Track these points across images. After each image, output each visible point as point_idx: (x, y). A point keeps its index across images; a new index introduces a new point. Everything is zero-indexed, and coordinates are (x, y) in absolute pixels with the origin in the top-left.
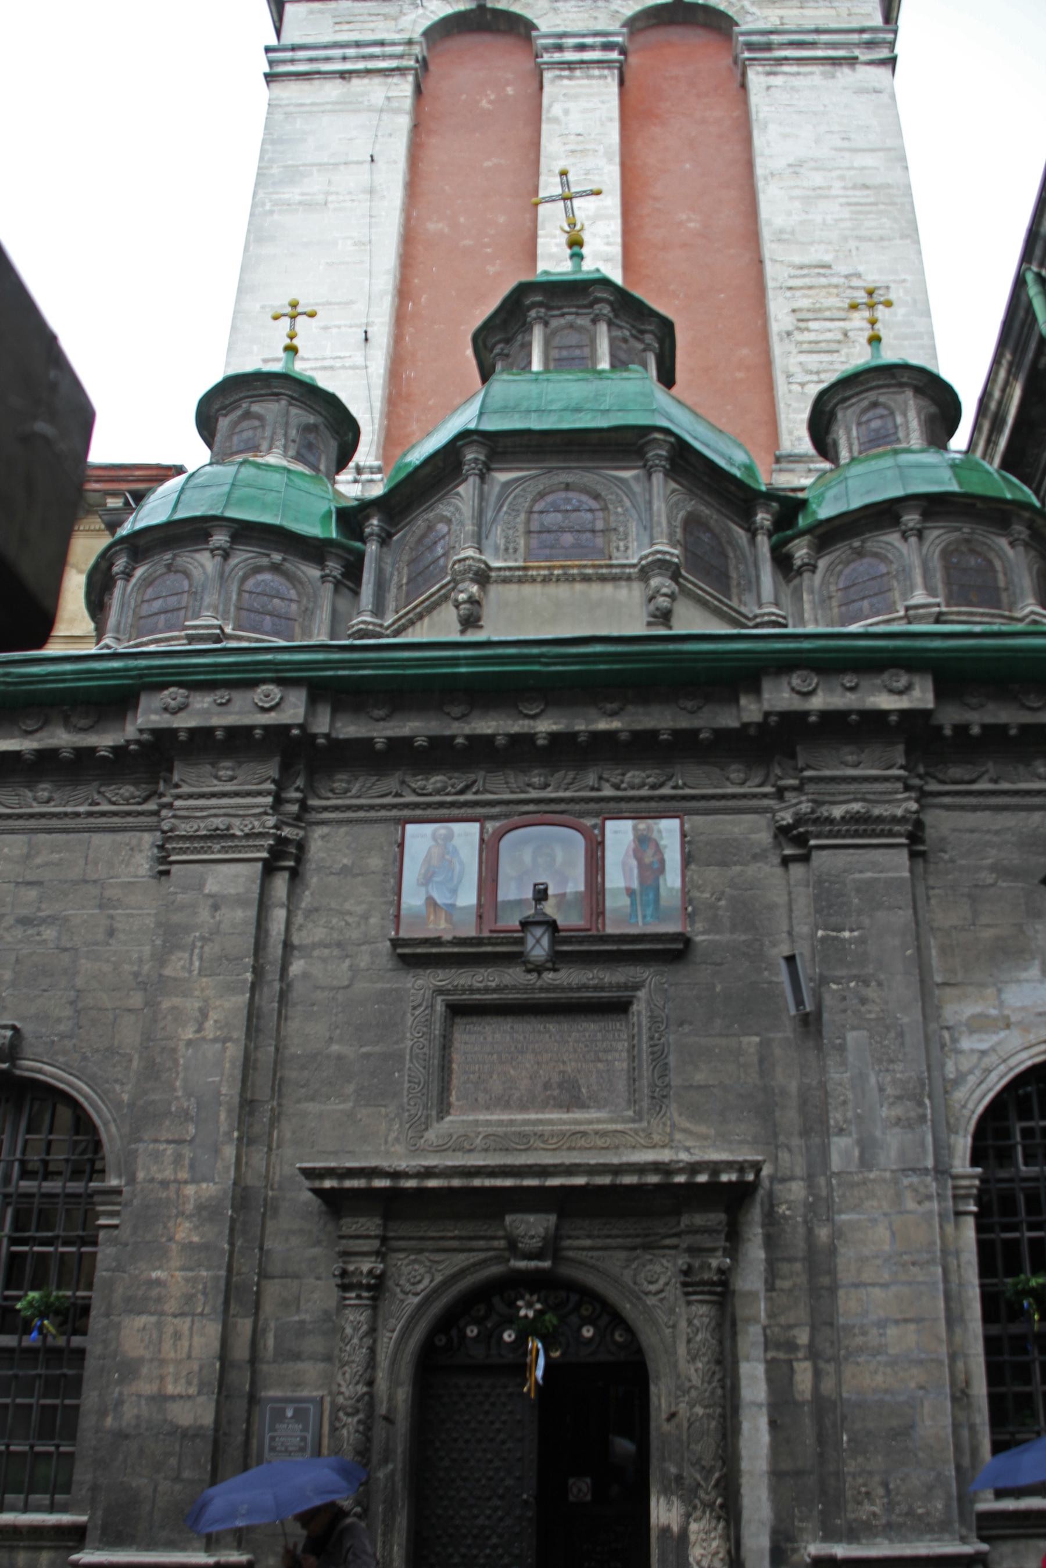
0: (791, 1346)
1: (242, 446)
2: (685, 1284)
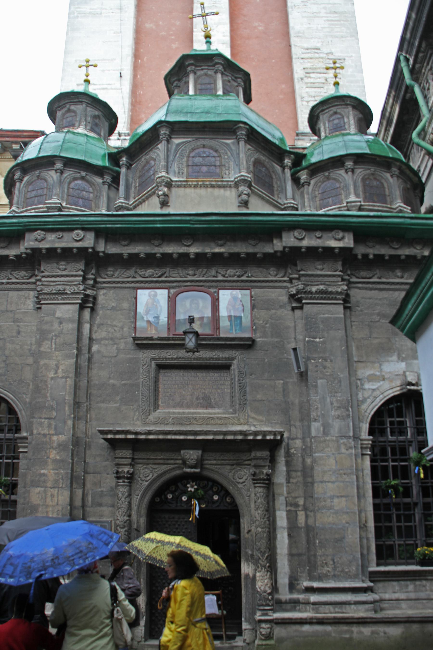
0: (296, 505)
1: (67, 124)
2: (253, 480)
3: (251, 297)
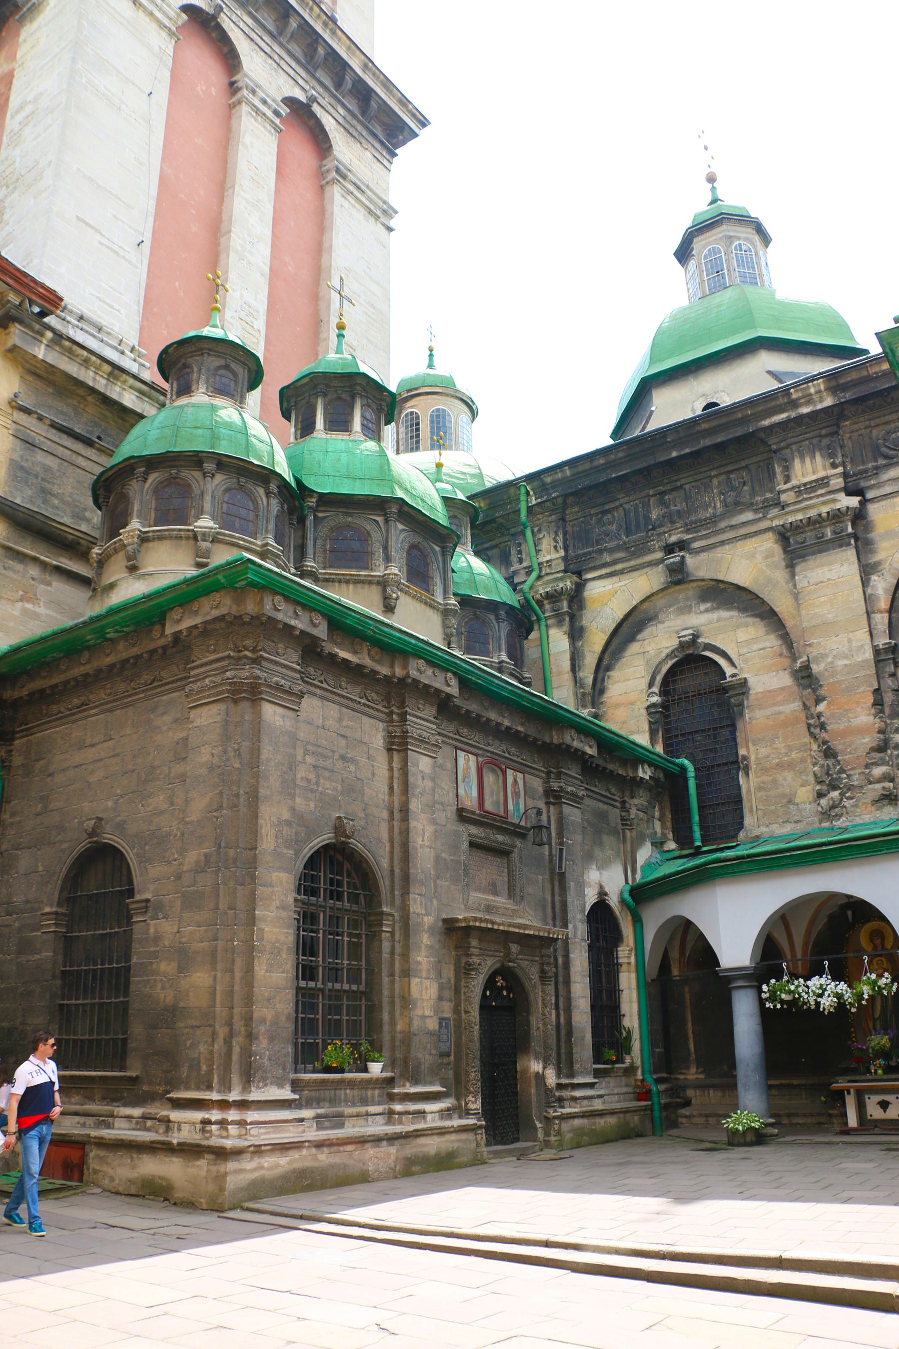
3: (524, 782)
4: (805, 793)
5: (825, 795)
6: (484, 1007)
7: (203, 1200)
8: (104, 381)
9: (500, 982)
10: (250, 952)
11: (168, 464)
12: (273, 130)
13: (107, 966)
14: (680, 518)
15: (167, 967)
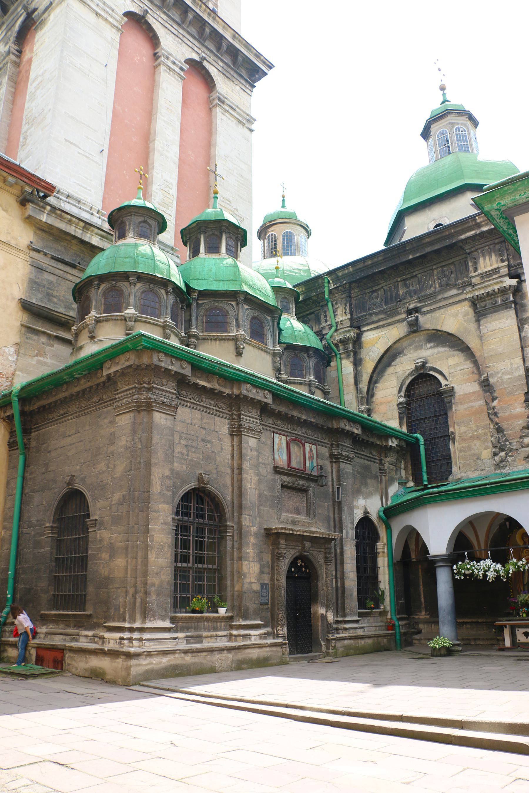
4: (486, 454)
5: (498, 454)
6: (289, 576)
7: (120, 680)
8: (80, 232)
9: (299, 563)
10: (146, 549)
11: (110, 279)
12: (179, 79)
13: (77, 555)
14: (415, 294)
15: (105, 556)
